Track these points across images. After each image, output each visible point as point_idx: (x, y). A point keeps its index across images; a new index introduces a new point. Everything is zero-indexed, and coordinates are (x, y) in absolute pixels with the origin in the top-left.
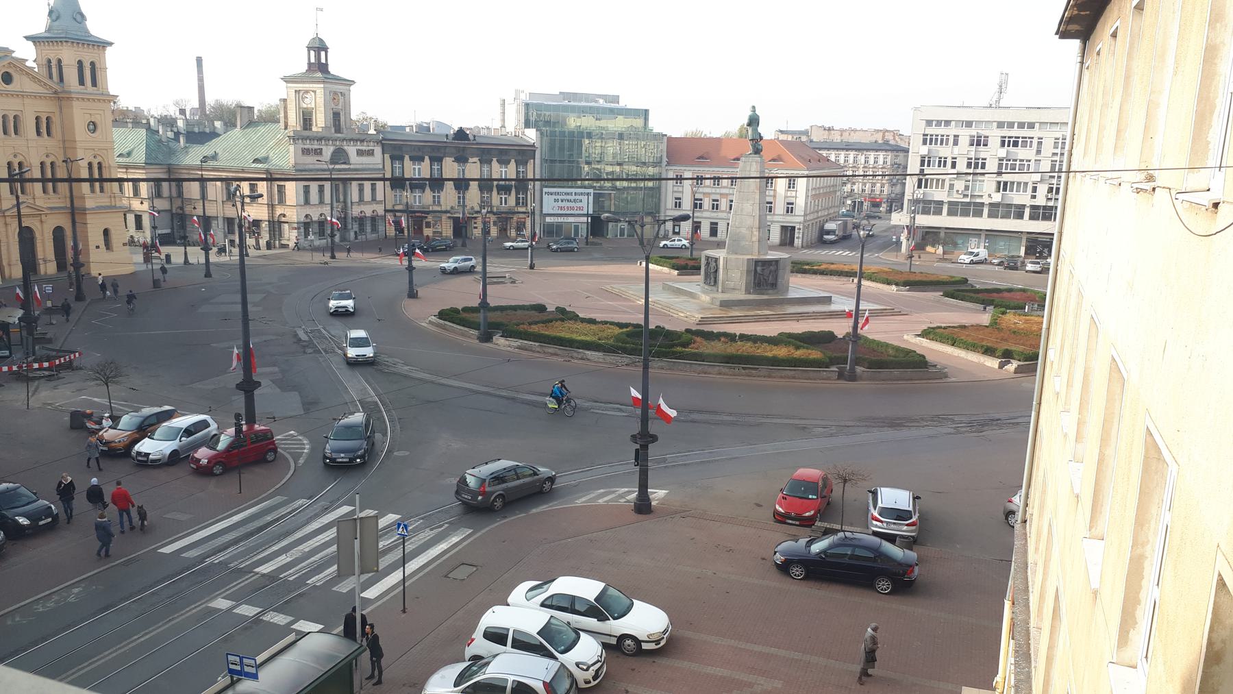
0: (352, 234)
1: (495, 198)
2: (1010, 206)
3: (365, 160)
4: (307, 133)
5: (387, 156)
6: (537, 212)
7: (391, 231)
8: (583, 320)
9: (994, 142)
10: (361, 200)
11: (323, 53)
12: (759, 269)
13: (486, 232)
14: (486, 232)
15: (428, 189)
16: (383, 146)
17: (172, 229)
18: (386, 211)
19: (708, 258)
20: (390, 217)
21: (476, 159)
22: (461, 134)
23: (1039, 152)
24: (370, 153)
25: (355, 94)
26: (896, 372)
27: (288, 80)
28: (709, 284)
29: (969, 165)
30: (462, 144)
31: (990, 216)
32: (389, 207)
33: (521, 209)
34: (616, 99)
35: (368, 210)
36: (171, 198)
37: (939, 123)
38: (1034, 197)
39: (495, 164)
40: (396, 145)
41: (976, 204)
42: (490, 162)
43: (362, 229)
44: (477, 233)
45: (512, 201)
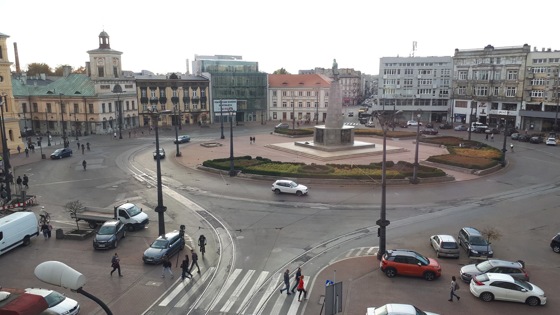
0: (125, 126)
1: (191, 105)
2: (423, 100)
3: (128, 90)
4: (102, 78)
5: (139, 88)
6: (211, 111)
7: (142, 123)
8: (275, 162)
9: (416, 72)
10: (128, 110)
11: (107, 39)
12: (343, 133)
13: (187, 122)
14: (187, 122)
15: (159, 103)
16: (137, 83)
17: (32, 128)
18: (139, 114)
19: (317, 129)
20: (142, 118)
21: (181, 88)
22: (174, 76)
23: (435, 76)
24: (131, 87)
25: (123, 58)
26: (434, 178)
27: (91, 52)
28: (319, 142)
29: (405, 82)
30: (174, 80)
32: (140, 112)
33: (203, 110)
34: (240, 58)
35: (131, 114)
36: (31, 113)
37: (391, 65)
38: (434, 95)
39: (190, 90)
40: (146, 83)
41: (445, 100)
42: (188, 89)
43: (129, 123)
44: (183, 122)
45: (199, 106)
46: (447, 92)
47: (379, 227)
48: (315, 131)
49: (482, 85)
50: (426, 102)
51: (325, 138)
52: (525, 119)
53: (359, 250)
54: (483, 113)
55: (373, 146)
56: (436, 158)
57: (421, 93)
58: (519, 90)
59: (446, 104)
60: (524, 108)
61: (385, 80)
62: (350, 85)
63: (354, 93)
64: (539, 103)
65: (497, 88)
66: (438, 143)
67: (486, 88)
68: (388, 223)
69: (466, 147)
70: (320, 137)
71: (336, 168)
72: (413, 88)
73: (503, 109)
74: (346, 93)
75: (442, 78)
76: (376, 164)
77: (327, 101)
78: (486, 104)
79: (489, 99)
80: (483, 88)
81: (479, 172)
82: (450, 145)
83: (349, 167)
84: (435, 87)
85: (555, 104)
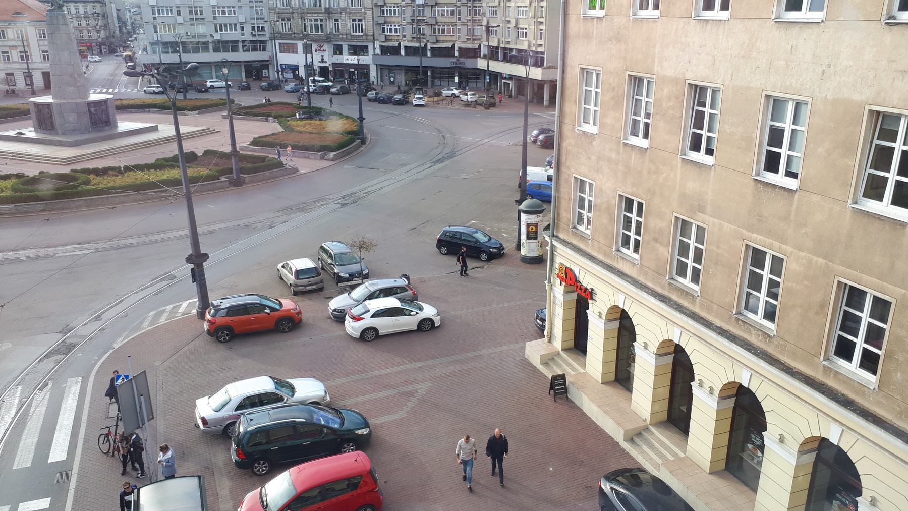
2: (227, 42)
12: (92, 110)
19: (37, 105)
26: (267, 173)
28: (46, 129)
29: (191, 12)
31: (214, 51)
38: (243, 34)
46: (263, 28)
47: (192, 266)
48: (33, 109)
49: (315, 16)
50: (232, 46)
51: (57, 120)
52: (381, 67)
53: (164, 311)
54: (323, 61)
55: (155, 129)
56: (264, 139)
57: (221, 30)
58: (368, 24)
59: (264, 49)
60: (378, 51)
61: (153, 7)
62: (86, 17)
63: (98, 31)
64: (396, 44)
65: (337, 20)
66: (263, 115)
67: (321, 20)
68: (205, 256)
69: (307, 118)
70: (45, 119)
71: (91, 176)
72: (205, 22)
73: (350, 54)
74: (81, 32)
75: (251, 4)
76: (165, 160)
77: (46, 49)
78: (326, 47)
79: (328, 39)
80: (316, 20)
81: (332, 155)
82: (282, 116)
83: (118, 171)
84: (242, 19)
85: (417, 45)
